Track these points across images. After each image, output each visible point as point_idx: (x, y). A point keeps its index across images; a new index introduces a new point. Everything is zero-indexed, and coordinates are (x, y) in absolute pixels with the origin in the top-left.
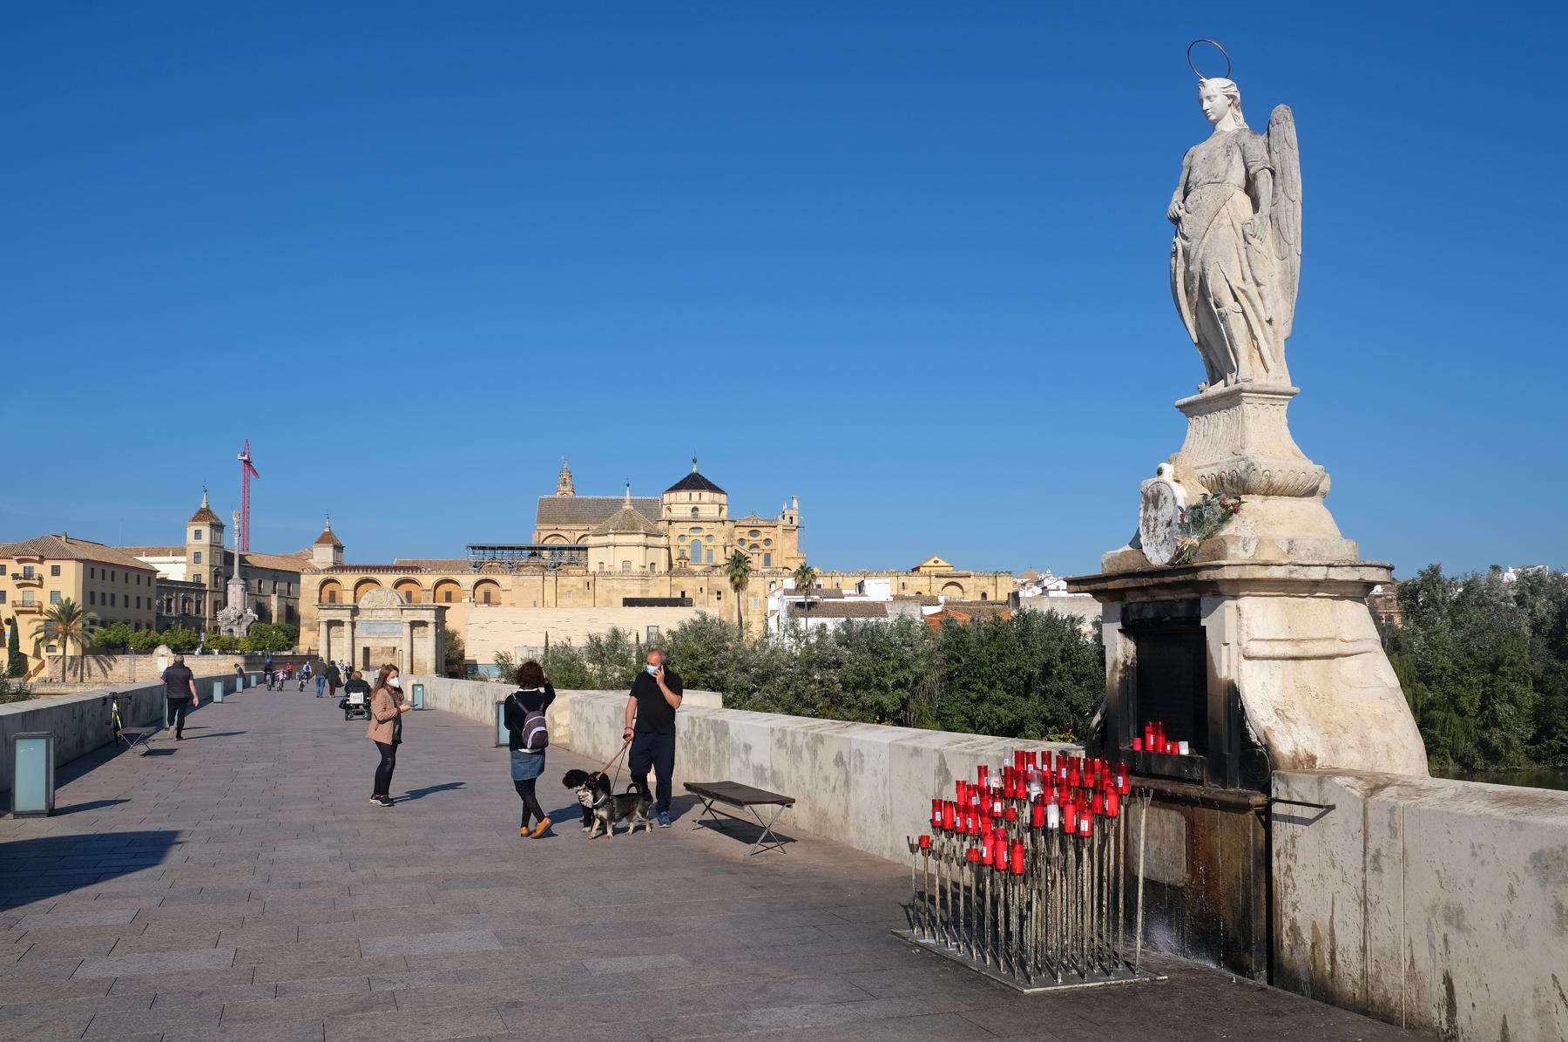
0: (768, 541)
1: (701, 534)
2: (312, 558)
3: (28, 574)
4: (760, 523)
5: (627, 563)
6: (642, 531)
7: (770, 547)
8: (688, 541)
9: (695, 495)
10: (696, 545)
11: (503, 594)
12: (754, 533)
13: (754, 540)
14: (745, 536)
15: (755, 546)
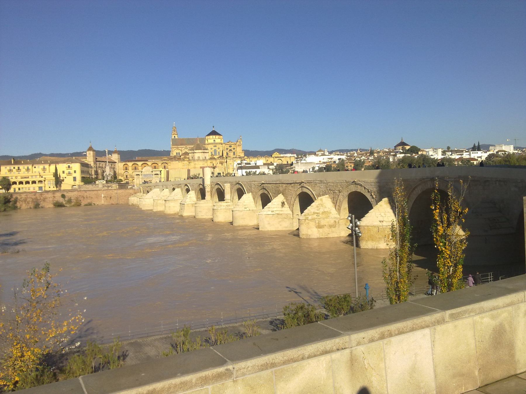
0: (234, 149)
1: (216, 147)
2: (112, 157)
3: (69, 167)
4: (232, 143)
5: (199, 157)
6: (202, 149)
7: (235, 150)
8: (213, 149)
9: (214, 136)
10: (215, 151)
11: (169, 166)
12: (230, 146)
13: (230, 148)
14: (228, 147)
15: (230, 150)
